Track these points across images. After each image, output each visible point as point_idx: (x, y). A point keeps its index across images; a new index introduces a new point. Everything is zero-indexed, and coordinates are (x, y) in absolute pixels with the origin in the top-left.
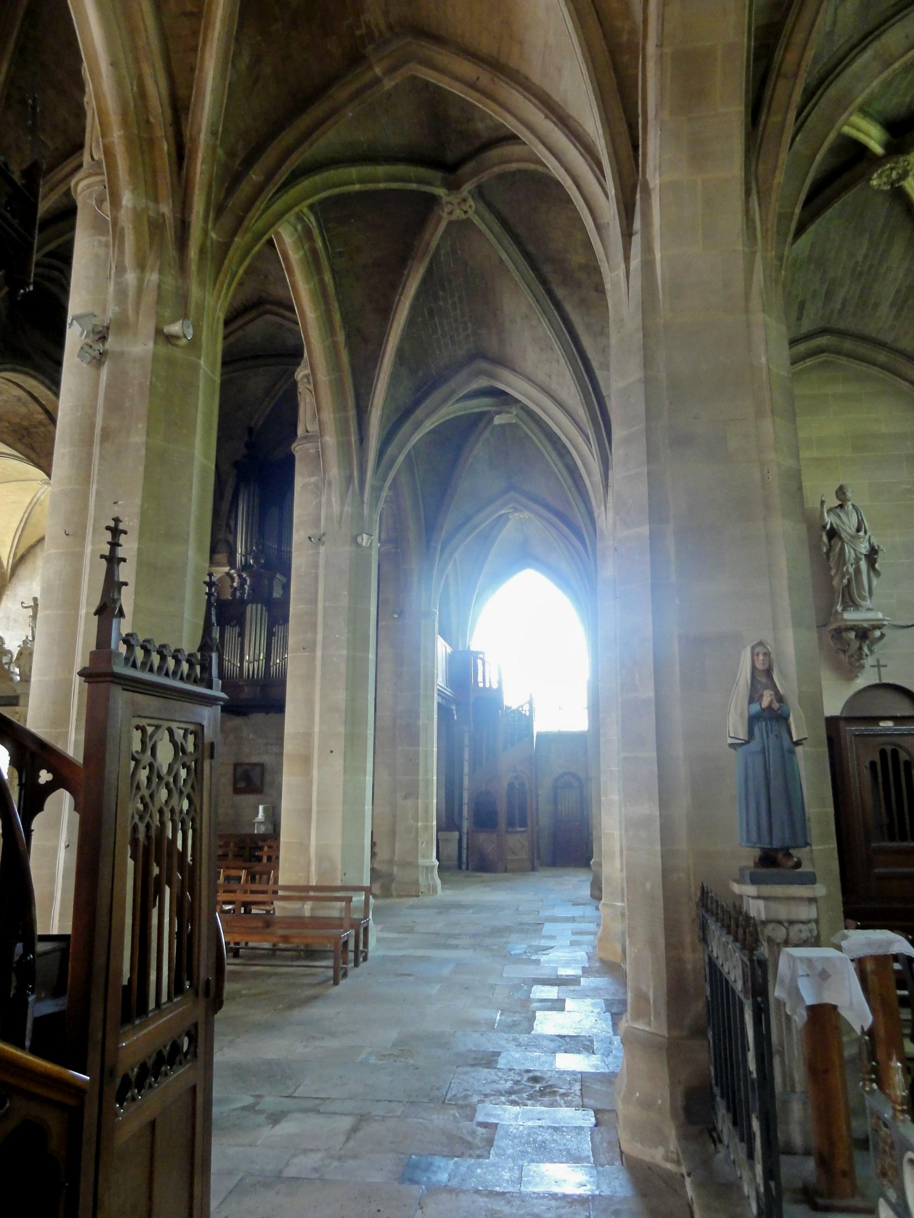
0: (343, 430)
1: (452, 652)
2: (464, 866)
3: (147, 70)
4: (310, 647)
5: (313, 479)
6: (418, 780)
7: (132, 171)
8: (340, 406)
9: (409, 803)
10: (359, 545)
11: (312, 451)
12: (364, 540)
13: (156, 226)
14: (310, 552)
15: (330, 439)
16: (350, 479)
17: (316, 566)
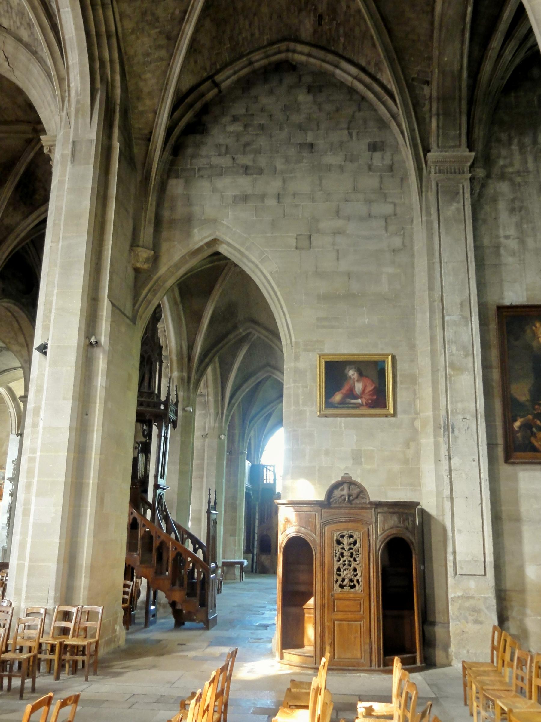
0: (216, 394)
1: (252, 466)
2: (254, 571)
3: (183, 342)
4: (201, 477)
5: (203, 412)
6: (236, 528)
7: (178, 367)
8: (216, 387)
9: (232, 538)
10: (220, 439)
11: (203, 401)
12: (223, 437)
13: (182, 379)
14: (202, 440)
15: (211, 399)
16: (218, 413)
17: (204, 446)
